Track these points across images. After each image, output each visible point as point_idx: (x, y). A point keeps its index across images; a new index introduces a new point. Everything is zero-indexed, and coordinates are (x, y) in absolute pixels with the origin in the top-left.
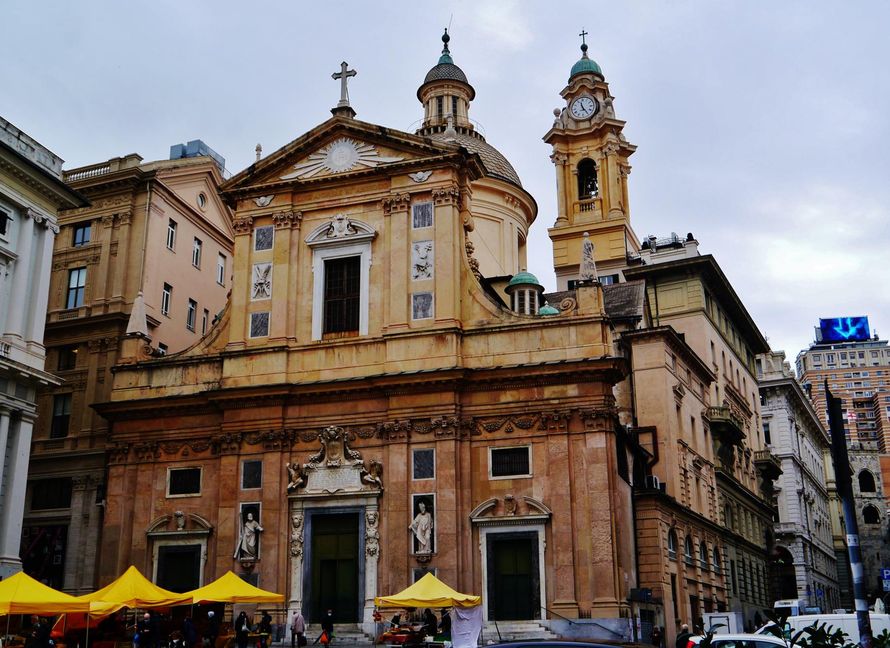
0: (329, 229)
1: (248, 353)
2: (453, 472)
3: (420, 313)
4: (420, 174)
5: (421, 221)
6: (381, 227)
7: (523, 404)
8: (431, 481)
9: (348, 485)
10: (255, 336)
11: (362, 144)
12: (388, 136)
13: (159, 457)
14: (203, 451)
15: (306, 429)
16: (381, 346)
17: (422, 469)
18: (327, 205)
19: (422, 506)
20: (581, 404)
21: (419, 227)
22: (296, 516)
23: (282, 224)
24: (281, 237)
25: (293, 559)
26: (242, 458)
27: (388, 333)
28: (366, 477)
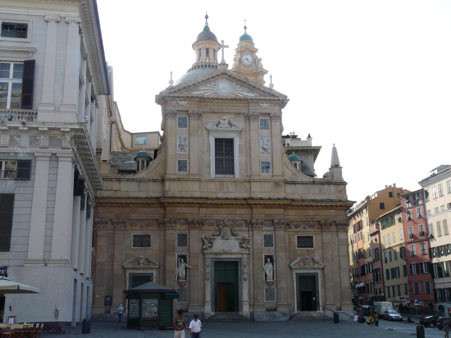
0: (218, 123)
1: (179, 180)
2: (283, 245)
3: (265, 170)
4: (265, 105)
5: (264, 126)
6: (243, 126)
7: (312, 217)
8: (272, 248)
9: (234, 248)
10: (180, 171)
11: (234, 84)
12: (250, 83)
13: (126, 227)
14: (152, 226)
15: (209, 220)
16: (248, 185)
17: (268, 243)
18: (216, 110)
19: (269, 260)
20: (336, 219)
21: (263, 129)
22: (207, 262)
23: (194, 116)
24: (194, 123)
25: (206, 282)
26: (176, 231)
27: (251, 178)
28: (243, 245)
